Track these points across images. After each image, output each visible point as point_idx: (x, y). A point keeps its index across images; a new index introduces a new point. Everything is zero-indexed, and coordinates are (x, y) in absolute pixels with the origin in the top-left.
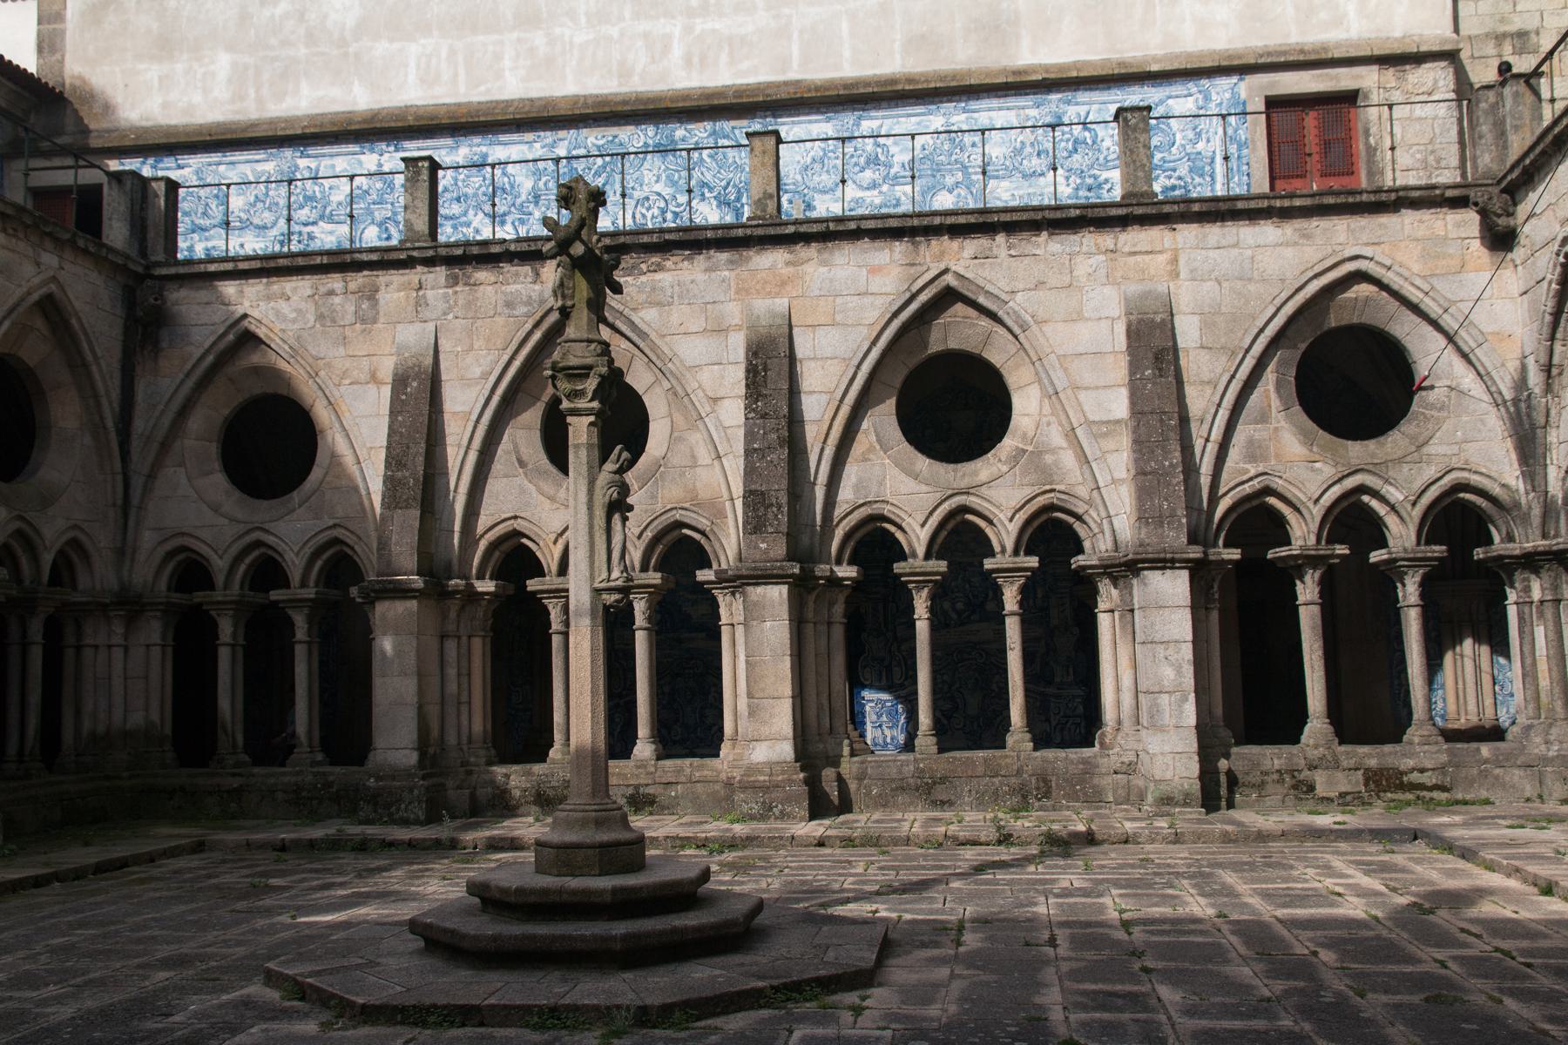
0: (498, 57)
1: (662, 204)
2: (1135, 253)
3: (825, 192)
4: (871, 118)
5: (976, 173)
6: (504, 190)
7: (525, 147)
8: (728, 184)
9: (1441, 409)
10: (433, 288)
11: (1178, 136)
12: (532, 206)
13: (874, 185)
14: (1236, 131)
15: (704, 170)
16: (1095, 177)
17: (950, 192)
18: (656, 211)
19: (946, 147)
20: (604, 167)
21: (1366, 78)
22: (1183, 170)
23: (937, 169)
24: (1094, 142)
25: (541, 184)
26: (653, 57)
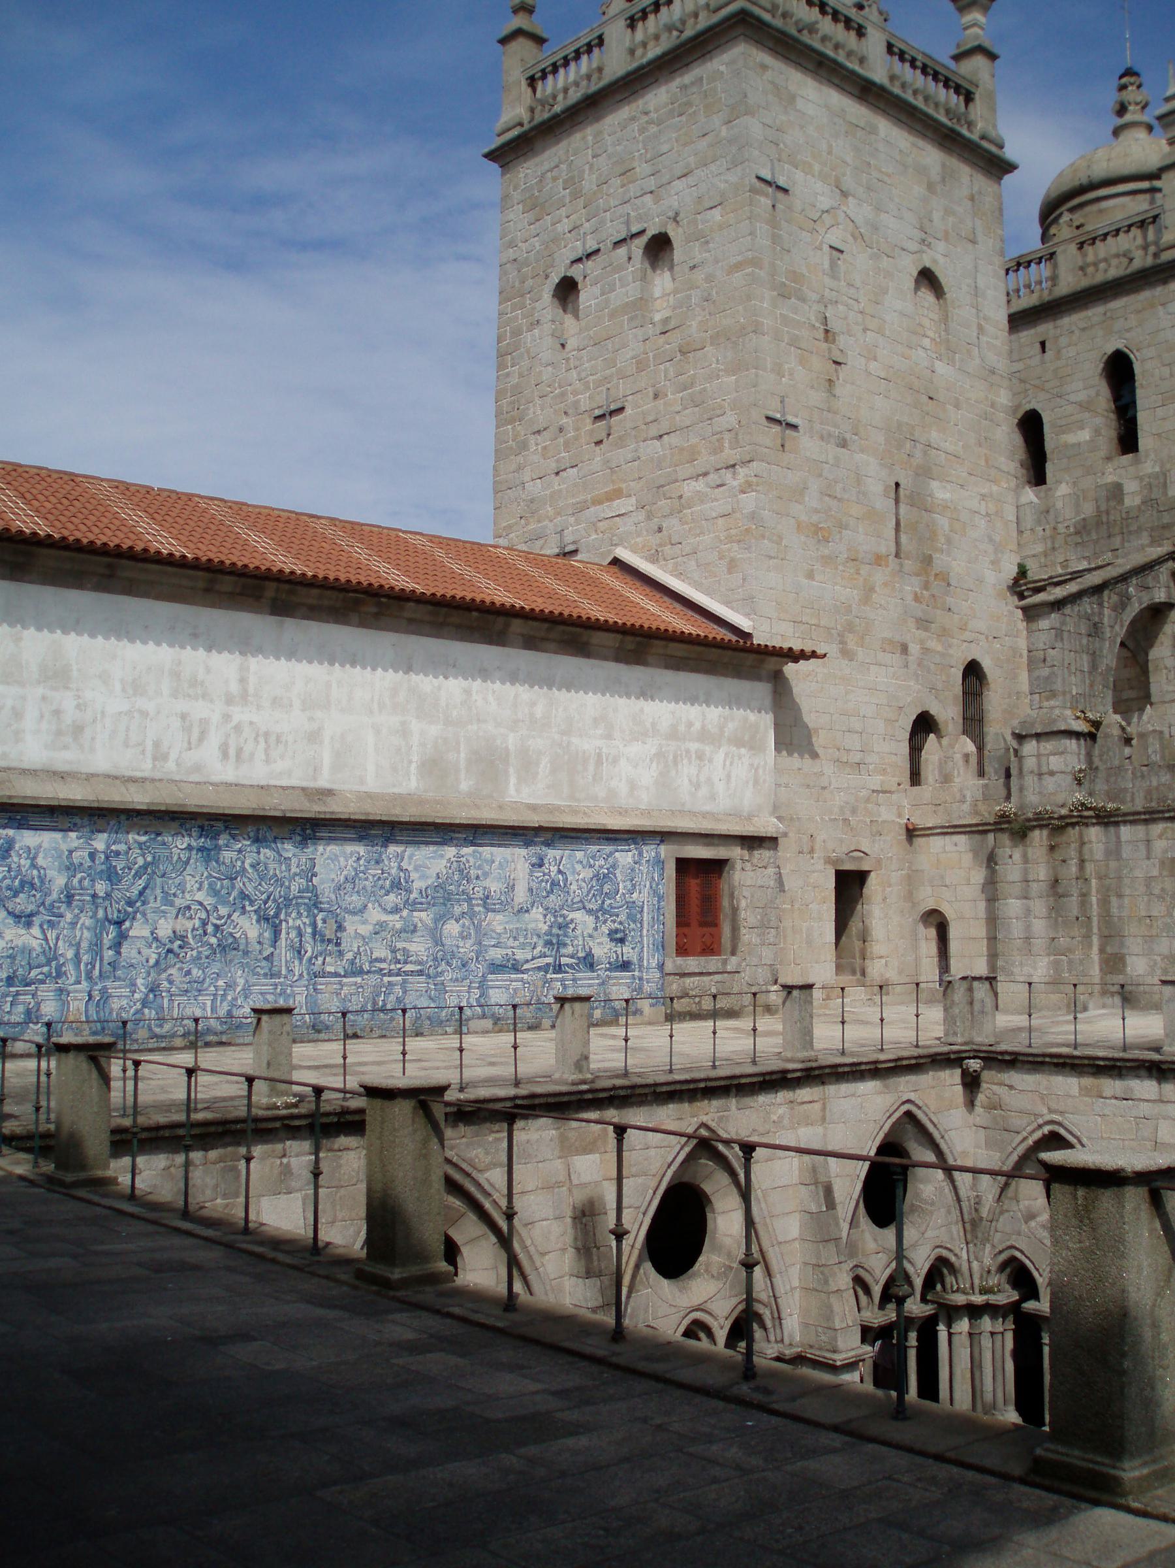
0: (18, 715)
1: (204, 916)
2: (803, 1103)
3: (354, 913)
4: (397, 842)
5: (478, 905)
6: (32, 885)
7: (58, 836)
8: (269, 898)
9: (932, 1204)
10: (297, 1156)
11: (621, 886)
12: (64, 906)
13: (396, 910)
14: (658, 885)
15: (246, 880)
16: (564, 917)
17: (457, 921)
18: (197, 923)
19: (456, 877)
20: (145, 867)
21: (735, 853)
22: (623, 917)
23: (448, 898)
24: (565, 885)
25: (75, 881)
26: (189, 743)
